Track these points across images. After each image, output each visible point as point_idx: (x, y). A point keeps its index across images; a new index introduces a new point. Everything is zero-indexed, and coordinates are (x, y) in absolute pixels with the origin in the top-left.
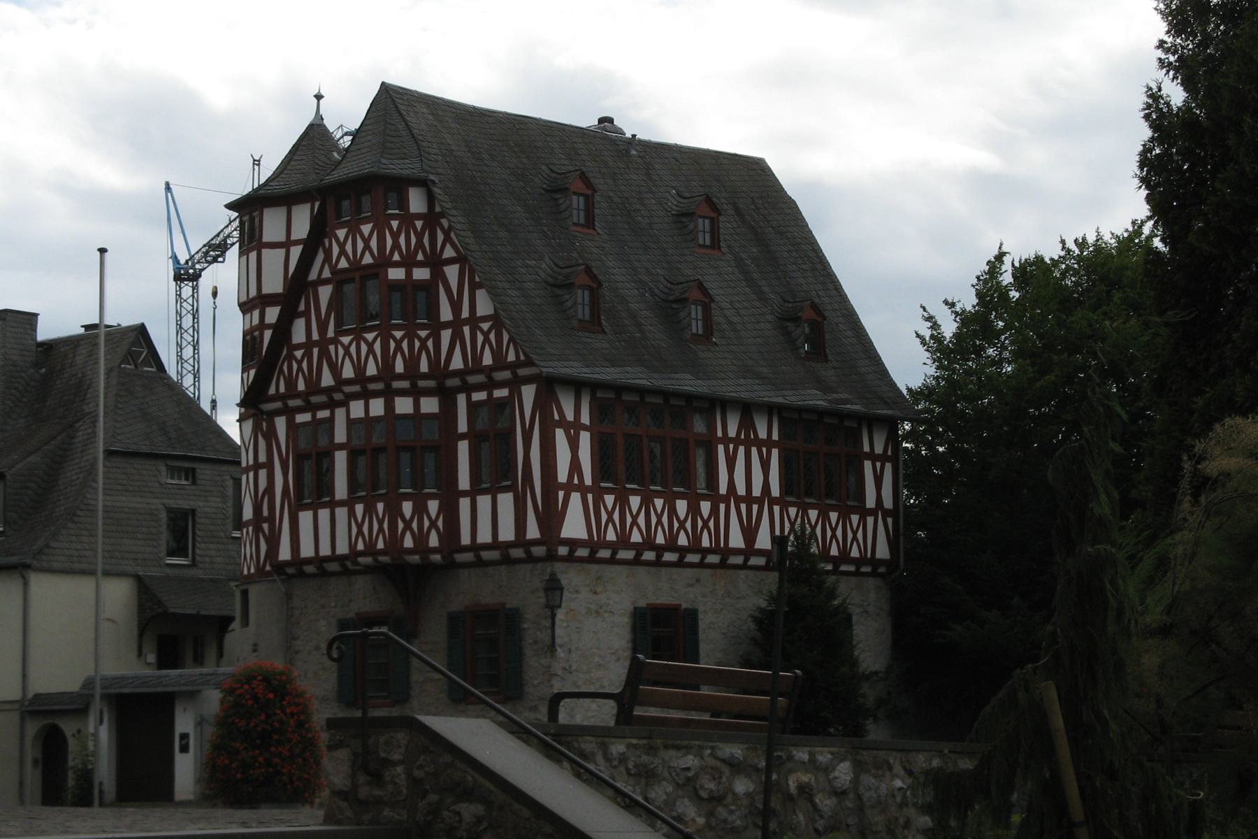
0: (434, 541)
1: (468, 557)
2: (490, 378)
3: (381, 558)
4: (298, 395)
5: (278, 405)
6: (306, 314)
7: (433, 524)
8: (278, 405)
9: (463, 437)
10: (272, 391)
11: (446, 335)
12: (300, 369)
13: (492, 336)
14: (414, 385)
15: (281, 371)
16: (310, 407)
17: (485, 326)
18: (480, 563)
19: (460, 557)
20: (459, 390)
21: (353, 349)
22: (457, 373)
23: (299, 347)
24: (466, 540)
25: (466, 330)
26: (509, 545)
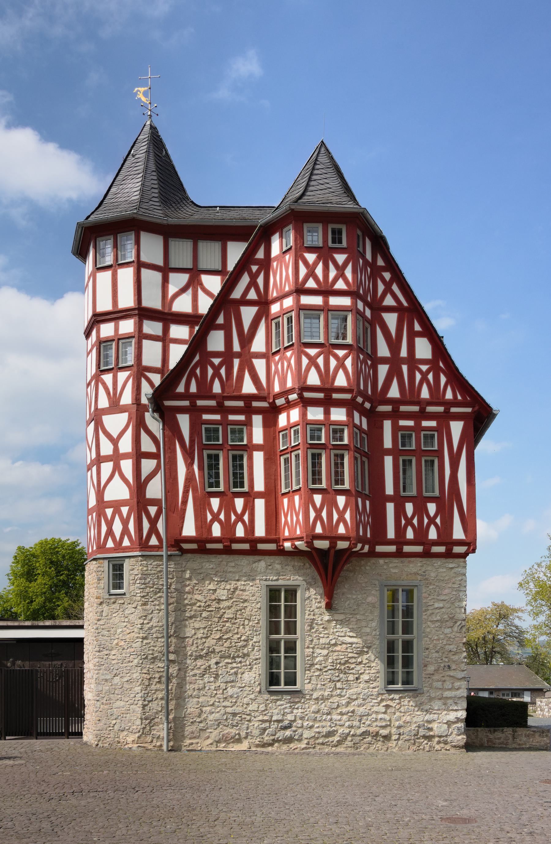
1: (392, 549)
2: (422, 410)
4: (213, 397)
8: (186, 403)
9: (388, 452)
10: (181, 389)
11: (383, 370)
15: (193, 374)
16: (220, 409)
18: (399, 554)
19: (380, 549)
22: (393, 402)
23: (216, 354)
24: (391, 534)
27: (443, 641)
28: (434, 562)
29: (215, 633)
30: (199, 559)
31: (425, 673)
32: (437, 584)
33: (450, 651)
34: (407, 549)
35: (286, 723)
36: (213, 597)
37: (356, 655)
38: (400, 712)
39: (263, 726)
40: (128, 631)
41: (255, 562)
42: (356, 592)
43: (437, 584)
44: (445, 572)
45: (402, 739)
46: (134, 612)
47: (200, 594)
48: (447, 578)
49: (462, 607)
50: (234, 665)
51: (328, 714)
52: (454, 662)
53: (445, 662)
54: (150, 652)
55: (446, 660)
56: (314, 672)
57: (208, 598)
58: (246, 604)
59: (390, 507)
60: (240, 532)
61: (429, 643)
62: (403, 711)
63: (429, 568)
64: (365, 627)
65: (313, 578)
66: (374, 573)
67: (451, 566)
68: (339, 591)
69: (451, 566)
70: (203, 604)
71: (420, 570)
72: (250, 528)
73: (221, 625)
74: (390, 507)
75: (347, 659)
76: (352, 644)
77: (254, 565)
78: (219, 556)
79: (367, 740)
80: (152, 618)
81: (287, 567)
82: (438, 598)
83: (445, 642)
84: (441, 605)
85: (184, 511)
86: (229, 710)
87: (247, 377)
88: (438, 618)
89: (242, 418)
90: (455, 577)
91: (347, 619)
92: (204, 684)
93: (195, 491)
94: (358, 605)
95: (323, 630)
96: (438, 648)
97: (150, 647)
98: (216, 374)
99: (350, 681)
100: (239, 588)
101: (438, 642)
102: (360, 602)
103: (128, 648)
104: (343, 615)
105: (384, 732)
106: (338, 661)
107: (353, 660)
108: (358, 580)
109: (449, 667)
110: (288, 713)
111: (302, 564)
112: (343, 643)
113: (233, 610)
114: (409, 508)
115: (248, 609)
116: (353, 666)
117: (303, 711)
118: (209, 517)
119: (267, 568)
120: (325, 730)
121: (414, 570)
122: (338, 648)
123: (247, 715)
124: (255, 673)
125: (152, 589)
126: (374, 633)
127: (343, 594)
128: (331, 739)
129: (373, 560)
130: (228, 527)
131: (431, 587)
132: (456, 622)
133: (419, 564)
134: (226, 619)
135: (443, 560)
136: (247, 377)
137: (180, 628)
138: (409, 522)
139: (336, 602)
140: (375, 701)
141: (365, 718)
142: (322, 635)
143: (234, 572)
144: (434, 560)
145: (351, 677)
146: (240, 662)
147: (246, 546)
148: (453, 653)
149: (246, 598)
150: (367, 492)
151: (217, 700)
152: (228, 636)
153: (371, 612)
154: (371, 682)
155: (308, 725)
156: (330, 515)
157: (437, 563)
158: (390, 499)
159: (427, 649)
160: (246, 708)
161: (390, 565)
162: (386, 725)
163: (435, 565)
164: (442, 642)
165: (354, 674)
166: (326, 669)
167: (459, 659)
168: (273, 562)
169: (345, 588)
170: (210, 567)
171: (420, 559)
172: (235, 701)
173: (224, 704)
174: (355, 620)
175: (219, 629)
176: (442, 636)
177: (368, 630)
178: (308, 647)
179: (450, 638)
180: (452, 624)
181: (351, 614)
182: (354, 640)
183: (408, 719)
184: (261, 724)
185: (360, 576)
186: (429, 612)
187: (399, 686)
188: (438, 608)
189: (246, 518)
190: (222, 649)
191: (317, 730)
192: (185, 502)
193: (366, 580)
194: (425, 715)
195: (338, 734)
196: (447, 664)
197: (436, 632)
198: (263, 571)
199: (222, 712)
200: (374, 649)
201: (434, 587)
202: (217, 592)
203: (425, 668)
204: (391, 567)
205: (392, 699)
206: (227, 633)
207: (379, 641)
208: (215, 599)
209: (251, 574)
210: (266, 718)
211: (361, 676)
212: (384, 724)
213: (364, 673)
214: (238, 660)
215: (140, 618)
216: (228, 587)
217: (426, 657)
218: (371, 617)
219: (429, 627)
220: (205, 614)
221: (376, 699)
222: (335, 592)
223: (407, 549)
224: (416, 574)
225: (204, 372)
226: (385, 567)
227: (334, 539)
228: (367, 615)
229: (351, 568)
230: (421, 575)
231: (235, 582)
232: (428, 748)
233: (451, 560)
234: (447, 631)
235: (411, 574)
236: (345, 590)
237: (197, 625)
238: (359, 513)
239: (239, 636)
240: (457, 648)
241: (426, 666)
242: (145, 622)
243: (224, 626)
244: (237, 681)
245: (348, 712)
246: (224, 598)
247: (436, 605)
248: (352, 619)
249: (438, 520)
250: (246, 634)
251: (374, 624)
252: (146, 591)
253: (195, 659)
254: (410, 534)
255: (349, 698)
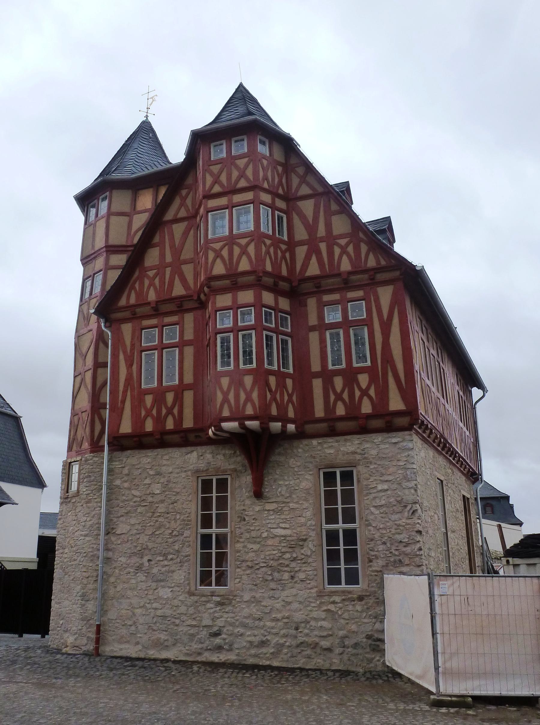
0: (291, 414)
1: (323, 426)
2: (346, 282)
3: (248, 423)
5: (127, 314)
6: (162, 244)
7: (290, 396)
10: (123, 302)
12: (151, 284)
13: (350, 249)
14: (276, 284)
15: (133, 287)
17: (343, 242)
19: (309, 428)
20: (310, 294)
21: (225, 253)
24: (319, 412)
25: (323, 246)
26: (368, 417)
27: (391, 529)
28: (373, 438)
29: (148, 529)
30: (138, 454)
31: (371, 569)
32: (379, 463)
33: (401, 541)
34: (341, 426)
35: (215, 629)
36: (148, 492)
37: (290, 550)
38: (344, 619)
39: (191, 632)
40: (76, 529)
41: (187, 454)
42: (288, 477)
43: (379, 463)
44: (387, 448)
45: (347, 654)
46: (80, 510)
47: (135, 489)
48: (390, 455)
49: (412, 488)
50: (166, 563)
51: (260, 619)
52: (407, 555)
53: (395, 555)
54: (90, 550)
55: (397, 553)
56: (244, 570)
57: (144, 493)
58: (178, 497)
59: (317, 384)
60: (170, 424)
61: (374, 533)
62: (347, 617)
63: (367, 445)
64: (299, 516)
65: (244, 466)
66: (307, 455)
67: (394, 440)
68: (270, 477)
69: (394, 440)
70: (138, 499)
71: (358, 448)
72: (179, 420)
73: (154, 520)
74: (317, 384)
75: (280, 555)
76: (285, 536)
77: (186, 457)
78: (155, 450)
79: (306, 653)
80: (94, 515)
81: (218, 456)
82: (381, 479)
83: (393, 531)
84: (385, 487)
85: (123, 409)
86: (159, 613)
87: (177, 282)
88: (383, 502)
89: (175, 318)
90: (400, 453)
91: (280, 508)
92: (137, 583)
93: (132, 390)
94: (291, 493)
95: (254, 521)
96: (386, 538)
97: (90, 545)
98: (151, 284)
99: (284, 580)
100: (172, 480)
101: (385, 532)
102: (292, 488)
103: (74, 546)
104: (274, 504)
105: (325, 644)
106: (272, 557)
107: (288, 556)
108: (290, 464)
109: (400, 561)
110: (218, 618)
111: (233, 452)
112: (276, 536)
113: (166, 504)
114: (338, 382)
115: (179, 503)
116: (287, 563)
117: (233, 615)
118: (143, 413)
119: (198, 458)
120: (256, 640)
121: (351, 449)
122: (270, 542)
123: (175, 618)
124: (185, 572)
125: (95, 487)
126: (309, 522)
127: (275, 481)
128: (264, 650)
129: (305, 442)
130: (159, 421)
131: (372, 467)
132: (405, 506)
133: (357, 442)
134: (159, 514)
135: (385, 435)
136: (177, 282)
137: (117, 525)
138: (339, 397)
139: (267, 490)
140: (313, 605)
141: (303, 625)
142: (252, 528)
143: (168, 465)
144: (373, 436)
145: (286, 576)
146: (172, 559)
147: (176, 438)
148: (404, 544)
149: (178, 490)
150: (291, 371)
151: (148, 601)
152: (161, 532)
153: (306, 500)
154: (308, 582)
155: (238, 632)
156: (237, 397)
157: (378, 439)
158: (316, 375)
159: (372, 540)
160: (175, 611)
161: (325, 446)
162: (328, 634)
163: (375, 441)
164: (390, 531)
165: (288, 572)
166: (257, 567)
167: (412, 551)
168: (204, 452)
169: (277, 474)
170: (147, 461)
171: (358, 436)
172: (164, 602)
173: (155, 605)
174: (288, 509)
175: (152, 524)
176: (388, 524)
177: (303, 520)
178: (238, 541)
179: (399, 525)
180: (400, 508)
181: (284, 502)
182: (288, 532)
183: (354, 627)
184: (189, 630)
185: (292, 460)
186: (371, 497)
187: (343, 586)
188: (381, 490)
189: (176, 411)
190: (153, 546)
191: (249, 639)
192: (123, 402)
193: (299, 464)
194: (375, 623)
195: (272, 645)
196: (397, 558)
197: (382, 519)
198: (194, 462)
199: (152, 615)
200: (311, 543)
201: (376, 466)
202: (152, 486)
203: (371, 564)
204: (326, 448)
205: (334, 602)
206: (159, 528)
207: (315, 532)
208: (150, 493)
209: (183, 466)
210: (194, 623)
211: (297, 575)
212: (325, 634)
213: (300, 570)
214: (170, 557)
215: (84, 516)
216: (162, 480)
217: (371, 550)
218: (306, 505)
219: (372, 513)
220: (140, 510)
221: (314, 602)
222: (266, 479)
223: (341, 426)
224: (354, 453)
225: (142, 284)
226: (319, 448)
227: (241, 419)
228: (300, 502)
229: (283, 452)
230: (360, 454)
231: (169, 475)
232: (381, 666)
233: (394, 434)
234: (395, 517)
235: (348, 453)
236: (277, 476)
237: (133, 521)
238: (270, 391)
239: (170, 532)
240: (408, 538)
241: (371, 561)
242: (88, 519)
243: (157, 521)
244: (168, 581)
245: (283, 618)
246: (158, 492)
247: (380, 487)
248: (285, 509)
249: (372, 392)
250: (177, 529)
251: (309, 514)
252: (91, 489)
253: (130, 557)
254: (340, 410)
255: (284, 601)
